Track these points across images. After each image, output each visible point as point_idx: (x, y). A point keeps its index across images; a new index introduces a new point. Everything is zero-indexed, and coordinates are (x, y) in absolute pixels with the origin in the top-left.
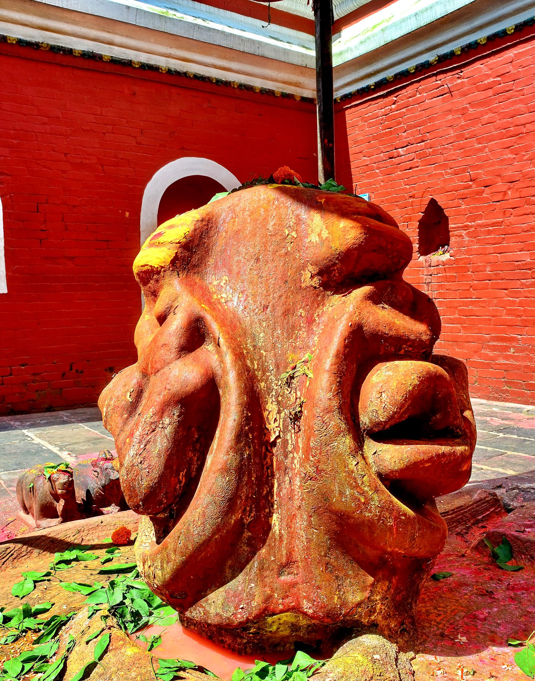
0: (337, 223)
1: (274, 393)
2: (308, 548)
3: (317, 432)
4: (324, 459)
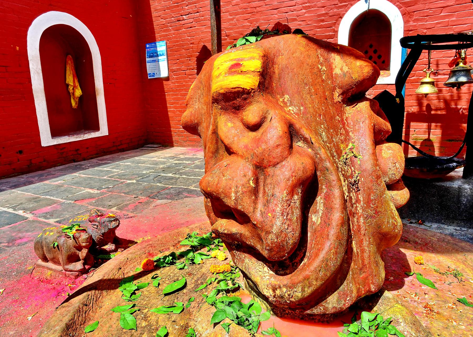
0: (354, 62)
1: (340, 170)
2: (369, 256)
3: (375, 191)
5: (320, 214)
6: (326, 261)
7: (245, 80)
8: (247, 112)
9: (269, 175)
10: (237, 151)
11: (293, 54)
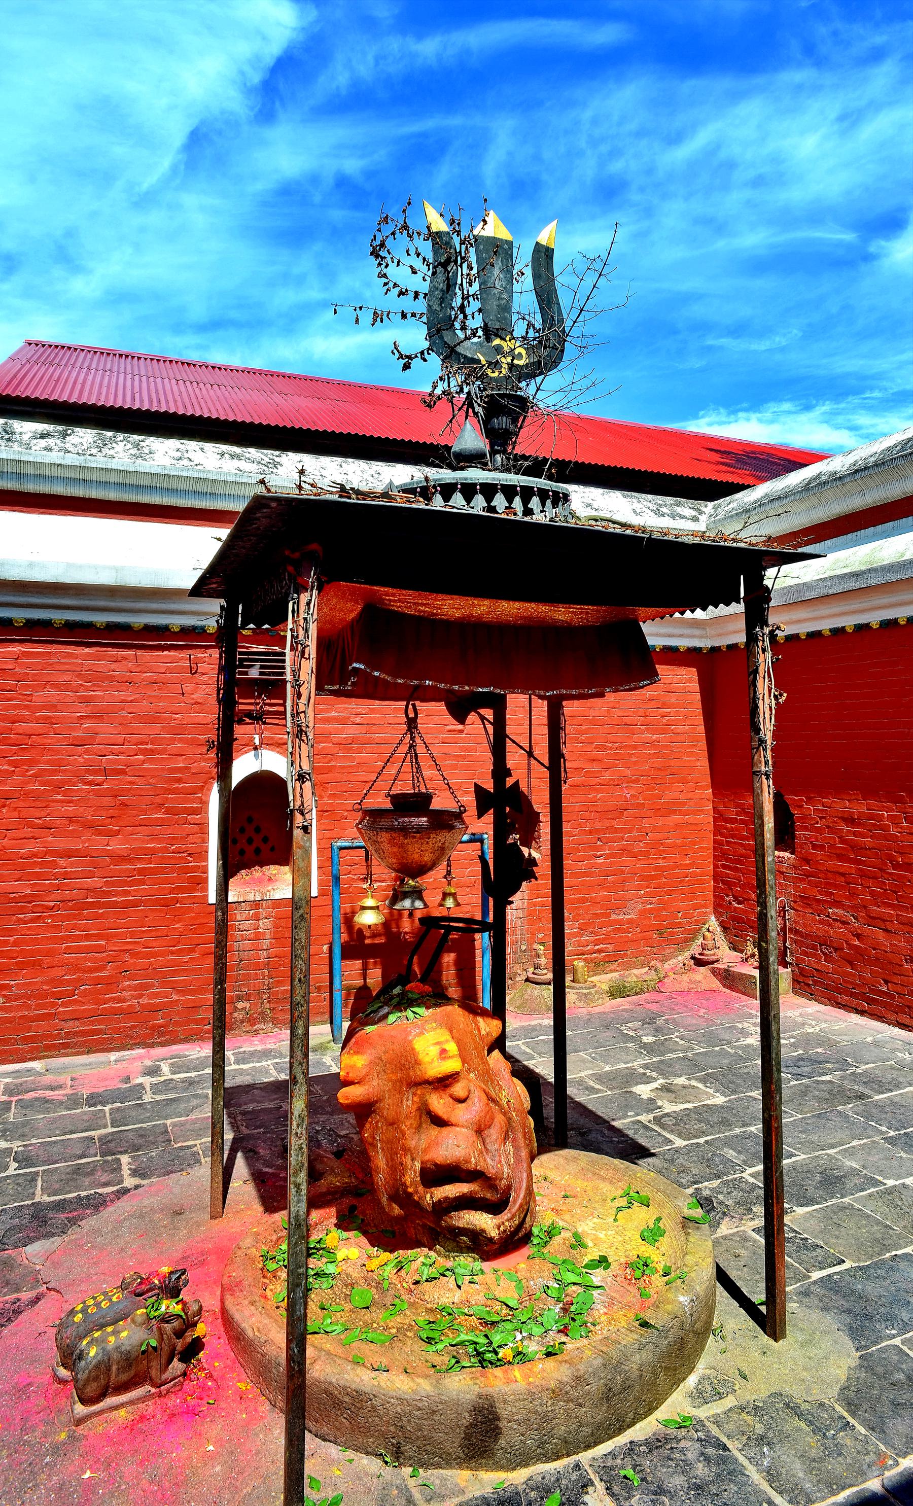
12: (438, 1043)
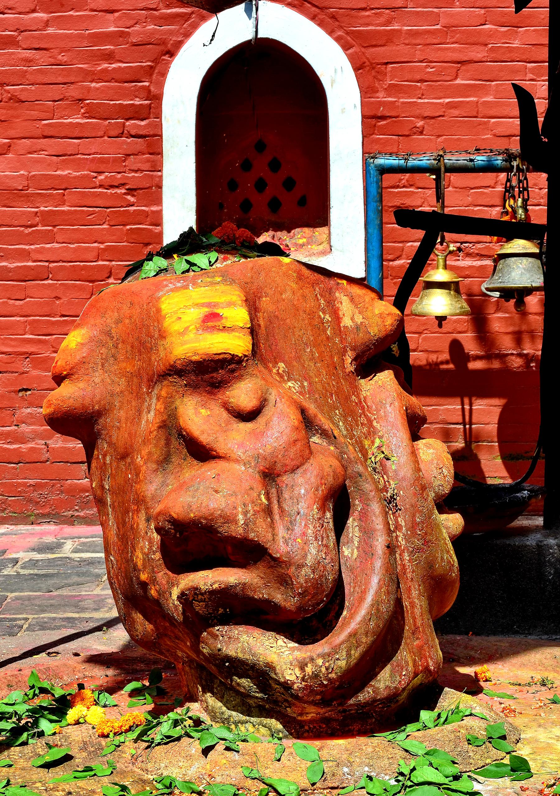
4: (429, 531)
5: (356, 544)
6: (376, 604)
7: (234, 342)
8: (236, 391)
9: (287, 485)
10: (226, 454)
11: (282, 294)
12: (209, 305)
